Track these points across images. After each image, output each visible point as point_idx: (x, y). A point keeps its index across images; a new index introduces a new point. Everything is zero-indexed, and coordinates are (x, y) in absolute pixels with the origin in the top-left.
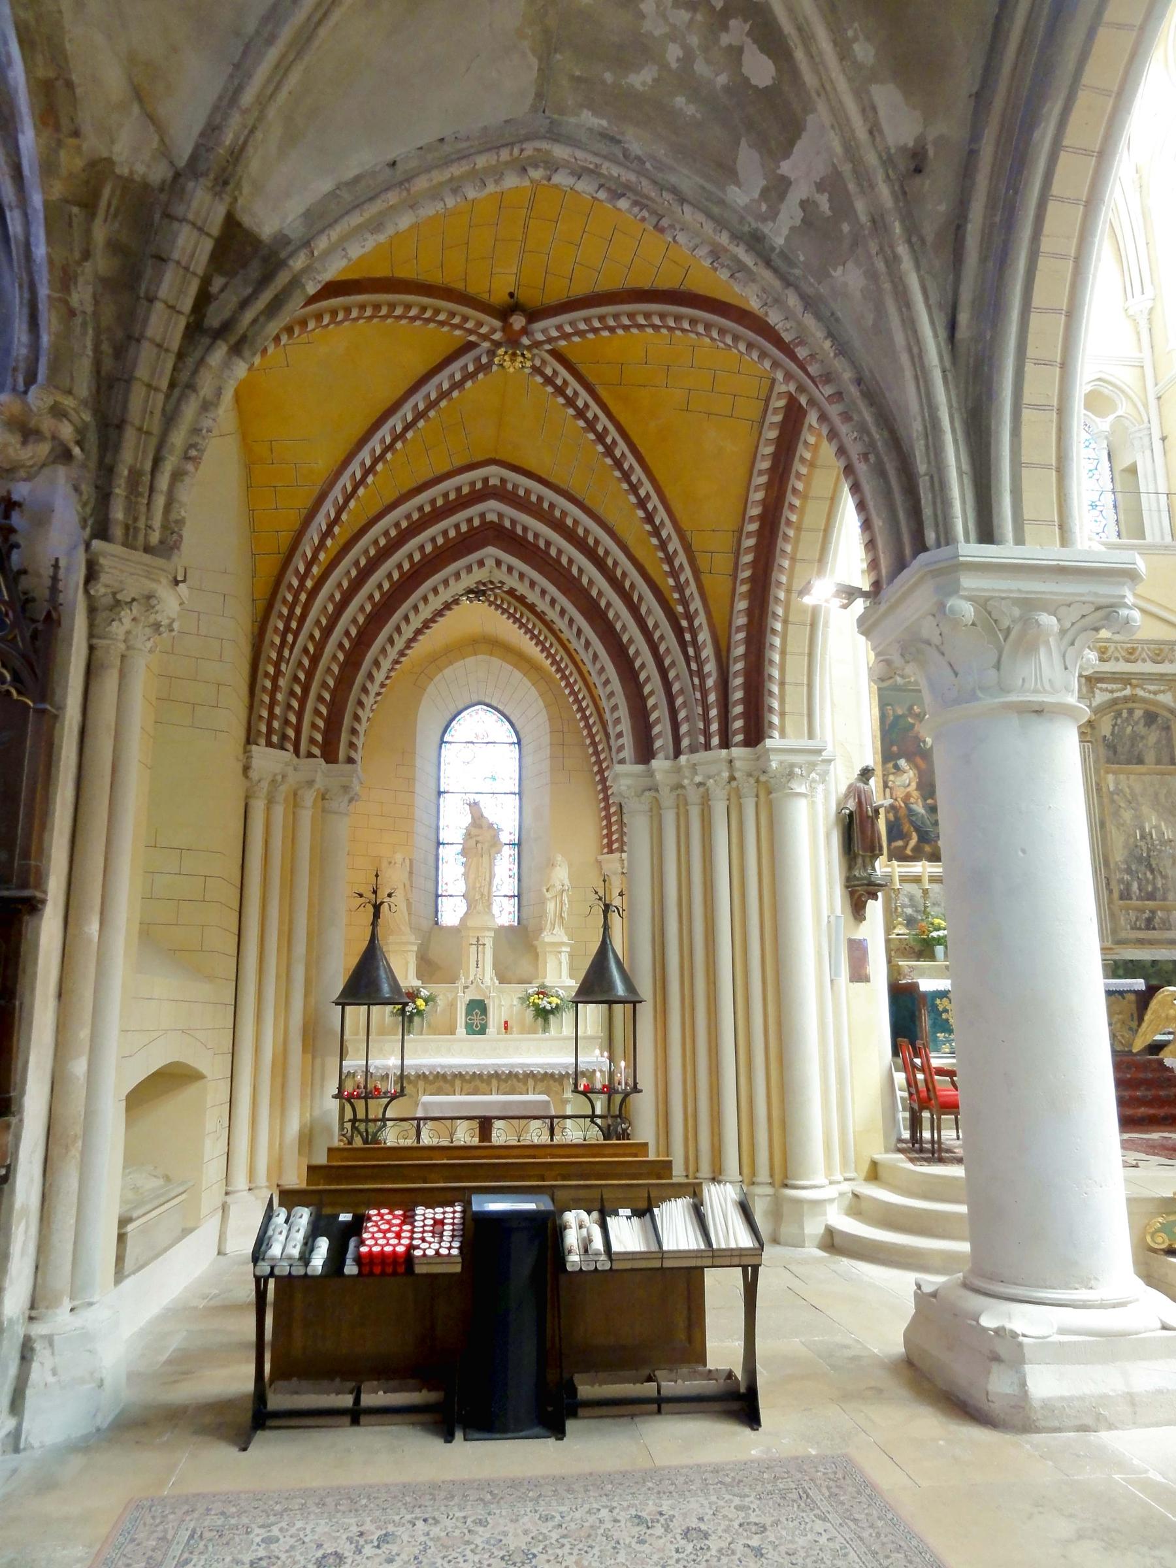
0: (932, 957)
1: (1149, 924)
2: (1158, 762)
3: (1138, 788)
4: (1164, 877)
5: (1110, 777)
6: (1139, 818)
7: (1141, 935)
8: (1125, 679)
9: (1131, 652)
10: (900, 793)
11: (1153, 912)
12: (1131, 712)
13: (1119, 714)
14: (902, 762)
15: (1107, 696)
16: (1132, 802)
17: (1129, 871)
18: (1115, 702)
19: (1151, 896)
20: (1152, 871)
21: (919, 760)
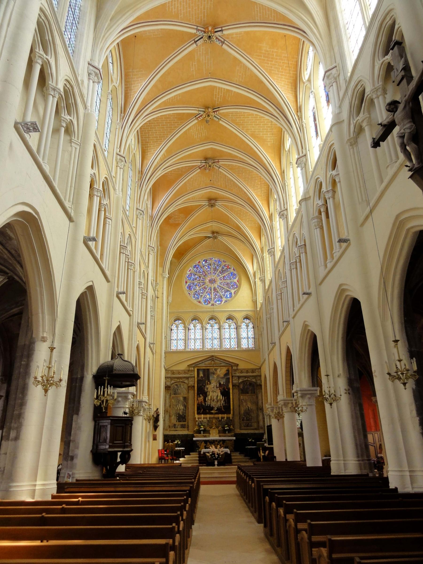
0: (200, 433)
1: (248, 426)
2: (251, 393)
3: (247, 398)
4: (251, 416)
5: (242, 396)
6: (247, 404)
7: (246, 428)
8: (245, 377)
9: (247, 371)
10: (200, 401)
11: (248, 423)
12: (247, 383)
13: (244, 384)
14: (201, 395)
15: (242, 380)
16: (246, 401)
17: (244, 415)
18: (243, 382)
19: (249, 420)
20: (249, 415)
21: (204, 395)
